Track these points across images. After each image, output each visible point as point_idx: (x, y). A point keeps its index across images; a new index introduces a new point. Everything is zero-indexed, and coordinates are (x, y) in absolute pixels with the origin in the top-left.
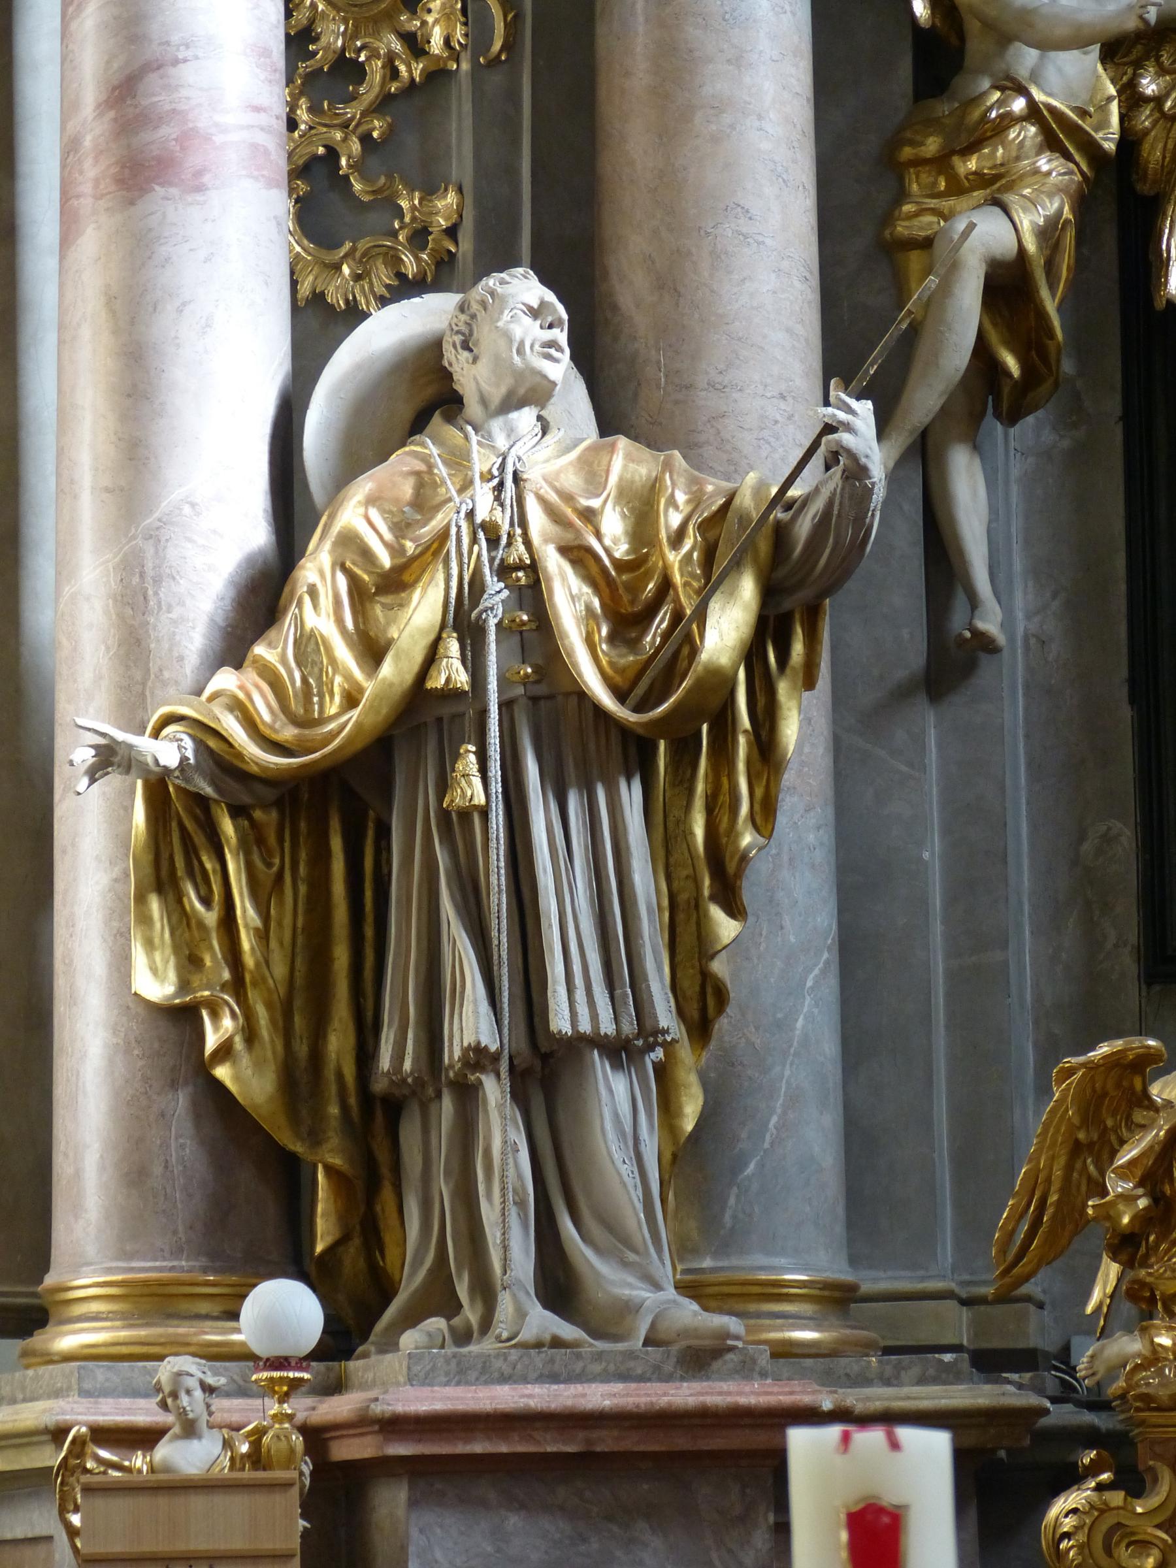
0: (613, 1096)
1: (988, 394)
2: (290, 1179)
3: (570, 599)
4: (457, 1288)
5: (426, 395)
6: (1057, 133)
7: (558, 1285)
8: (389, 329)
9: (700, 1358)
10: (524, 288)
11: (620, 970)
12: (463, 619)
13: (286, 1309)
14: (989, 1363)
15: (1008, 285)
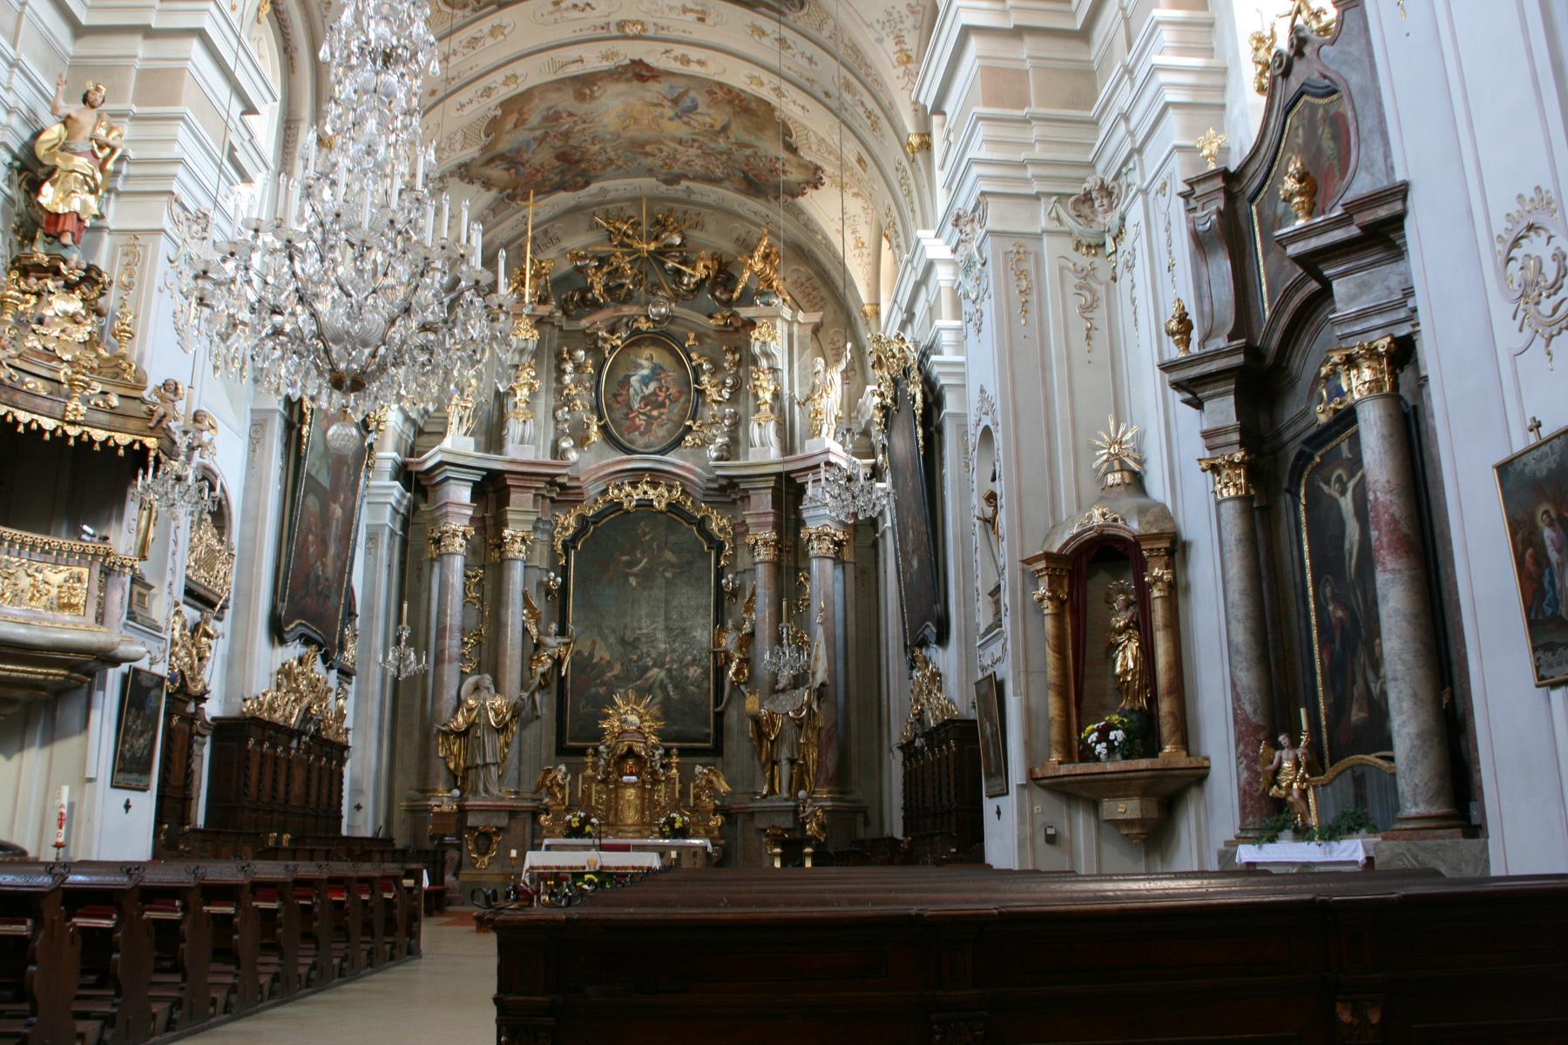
0: (493, 769)
1: (540, 687)
2: (456, 777)
3: (491, 715)
4: (476, 793)
5: (477, 688)
6: (550, 657)
7: (486, 791)
8: (472, 680)
9: (502, 799)
10: (487, 676)
11: (494, 755)
12: (479, 715)
13: (456, 792)
14: (534, 800)
15: (543, 675)
